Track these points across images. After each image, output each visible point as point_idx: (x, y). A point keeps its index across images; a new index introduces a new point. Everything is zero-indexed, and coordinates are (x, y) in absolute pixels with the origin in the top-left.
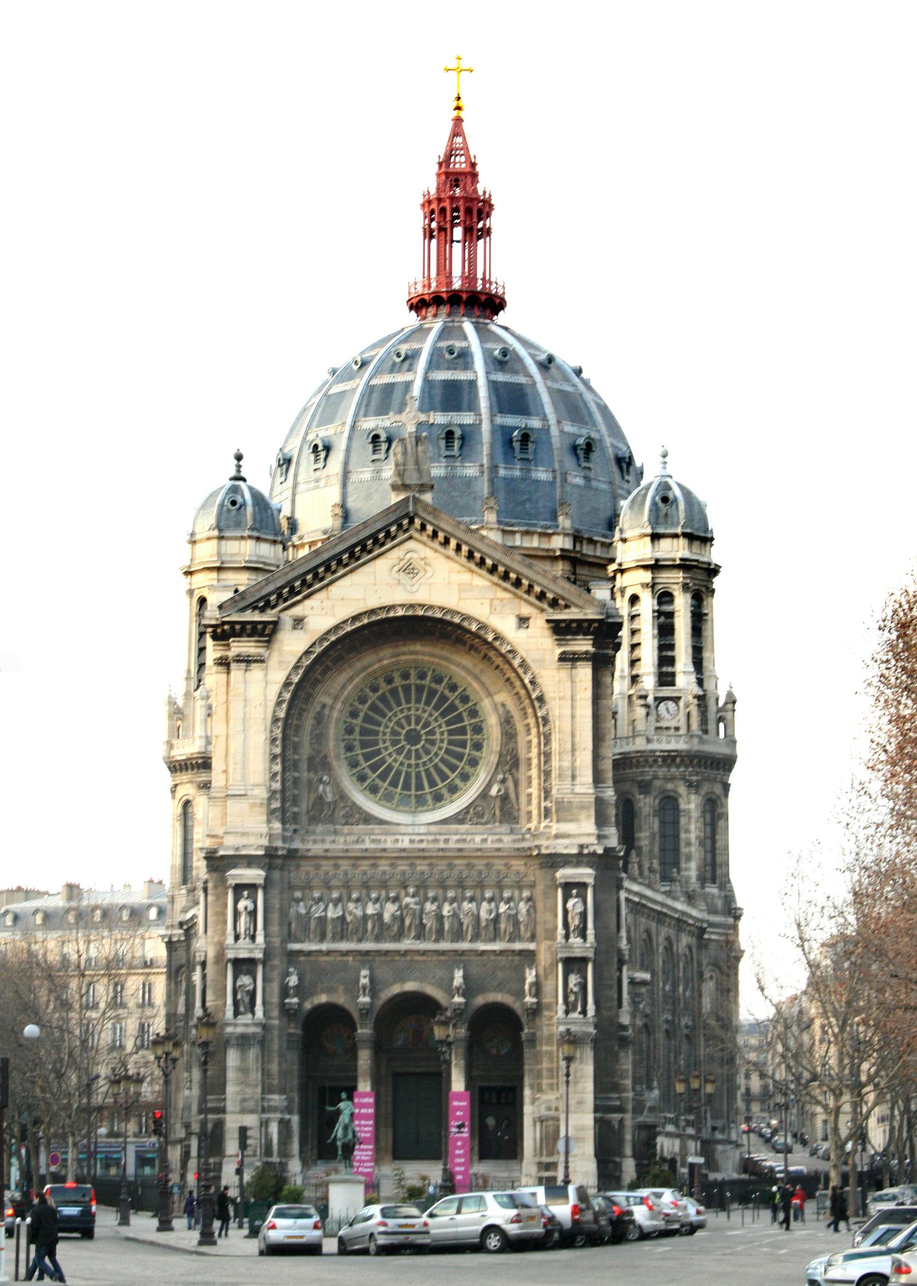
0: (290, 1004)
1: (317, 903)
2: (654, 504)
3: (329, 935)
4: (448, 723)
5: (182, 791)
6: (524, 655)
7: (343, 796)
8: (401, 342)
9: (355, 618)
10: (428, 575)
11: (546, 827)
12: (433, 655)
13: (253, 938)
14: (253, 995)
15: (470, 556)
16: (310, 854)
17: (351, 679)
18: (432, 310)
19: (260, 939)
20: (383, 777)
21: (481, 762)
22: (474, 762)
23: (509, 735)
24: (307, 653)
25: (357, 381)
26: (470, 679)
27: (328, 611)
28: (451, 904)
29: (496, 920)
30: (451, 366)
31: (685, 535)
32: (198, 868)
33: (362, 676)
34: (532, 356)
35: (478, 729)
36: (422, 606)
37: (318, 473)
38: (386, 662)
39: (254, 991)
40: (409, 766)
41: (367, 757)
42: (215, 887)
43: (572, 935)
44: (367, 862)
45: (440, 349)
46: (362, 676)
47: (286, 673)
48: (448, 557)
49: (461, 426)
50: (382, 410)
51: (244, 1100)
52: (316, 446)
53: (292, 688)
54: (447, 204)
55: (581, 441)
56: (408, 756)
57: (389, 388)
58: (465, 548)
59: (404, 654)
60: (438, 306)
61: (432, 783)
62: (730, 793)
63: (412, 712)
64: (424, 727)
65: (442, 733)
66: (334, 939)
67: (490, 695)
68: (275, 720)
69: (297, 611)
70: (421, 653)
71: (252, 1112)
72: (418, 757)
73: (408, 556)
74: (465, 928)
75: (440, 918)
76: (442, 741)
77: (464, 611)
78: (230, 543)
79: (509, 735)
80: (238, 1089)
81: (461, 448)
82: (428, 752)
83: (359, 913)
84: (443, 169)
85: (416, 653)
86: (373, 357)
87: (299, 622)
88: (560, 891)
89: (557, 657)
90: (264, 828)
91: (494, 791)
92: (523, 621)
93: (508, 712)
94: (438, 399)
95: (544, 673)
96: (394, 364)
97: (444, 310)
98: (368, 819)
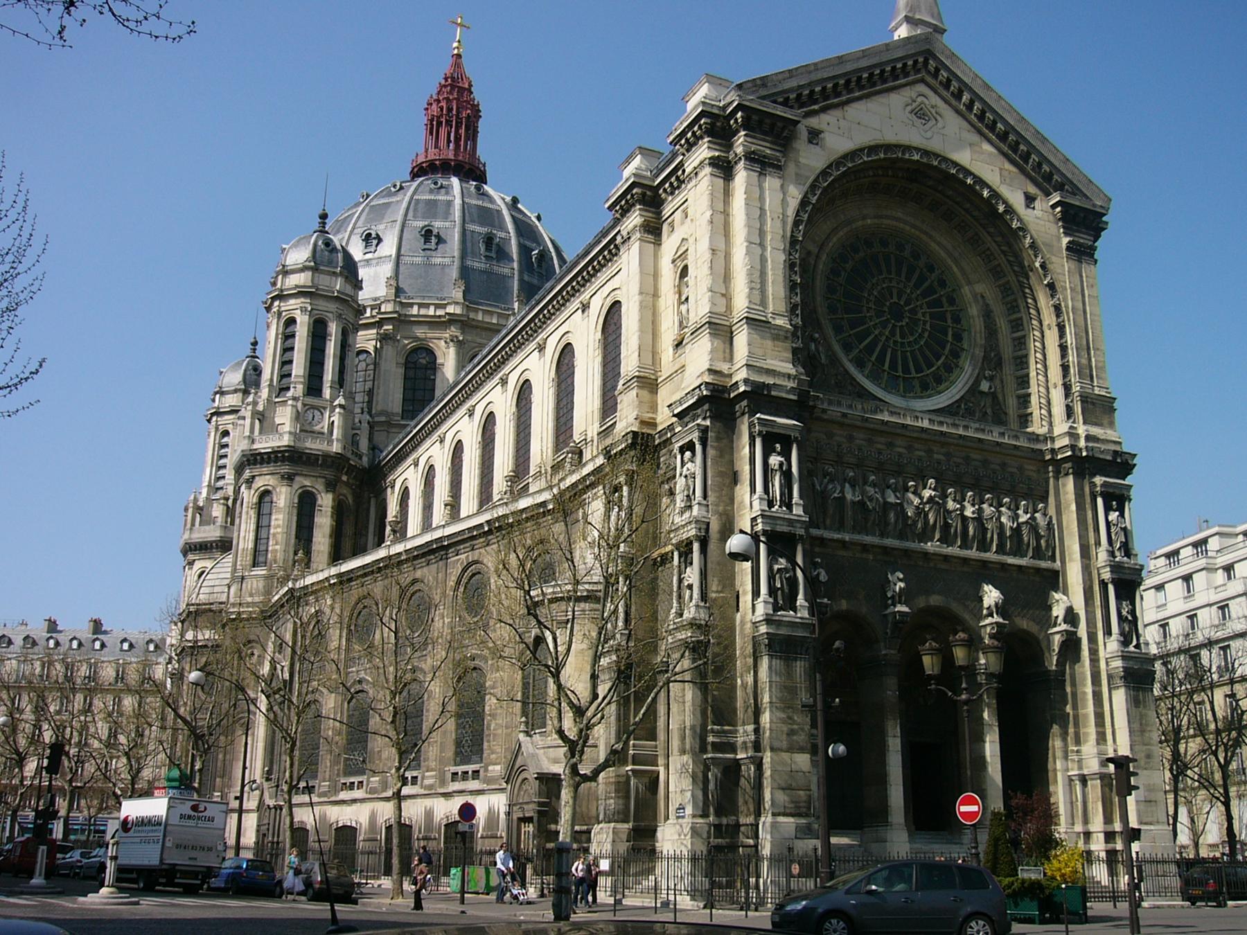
1: (831, 481)
3: (849, 522)
5: (260, 483)
6: (1035, 236)
7: (834, 360)
9: (873, 149)
10: (940, 125)
11: (1071, 427)
12: (913, 226)
13: (790, 507)
14: (793, 582)
15: (981, 117)
16: (826, 417)
17: (834, 230)
19: (798, 511)
20: (870, 349)
21: (963, 355)
22: (956, 354)
23: (991, 331)
24: (824, 173)
26: (949, 262)
28: (973, 505)
29: (1017, 531)
33: (845, 230)
35: (957, 320)
36: (937, 155)
37: (369, 256)
38: (869, 221)
40: (895, 342)
42: (718, 439)
43: (1117, 553)
44: (882, 440)
46: (845, 230)
47: (805, 188)
48: (958, 112)
51: (791, 733)
52: (370, 235)
53: (809, 208)
58: (977, 106)
59: (887, 217)
63: (894, 284)
64: (908, 303)
66: (854, 530)
67: (969, 283)
68: (793, 242)
69: (814, 122)
70: (900, 219)
71: (801, 750)
72: (902, 337)
73: (920, 99)
75: (964, 519)
76: (925, 323)
77: (977, 173)
78: (322, 276)
79: (991, 331)
80: (783, 716)
82: (912, 334)
85: (898, 219)
87: (814, 136)
88: (1100, 501)
89: (1064, 246)
90: (788, 368)
91: (985, 386)
92: (1030, 200)
93: (987, 305)
95: (1054, 259)
98: (863, 394)
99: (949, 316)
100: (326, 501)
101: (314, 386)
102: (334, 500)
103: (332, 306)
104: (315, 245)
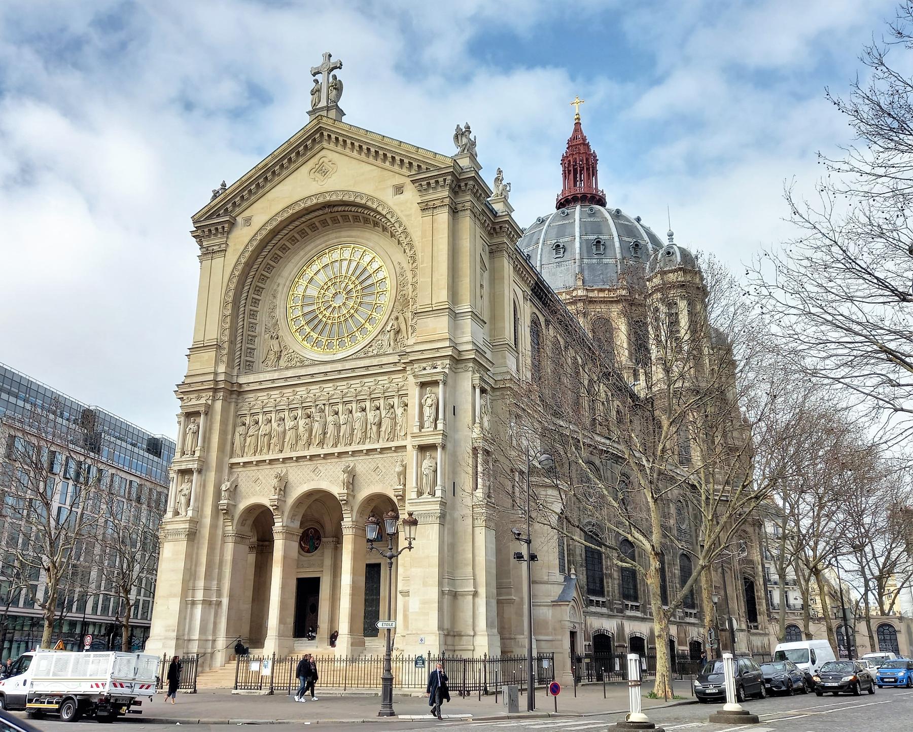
0: (223, 505)
27: (265, 212)
31: (680, 269)
47: (237, 257)
69: (247, 214)
83: (281, 429)
87: (248, 221)
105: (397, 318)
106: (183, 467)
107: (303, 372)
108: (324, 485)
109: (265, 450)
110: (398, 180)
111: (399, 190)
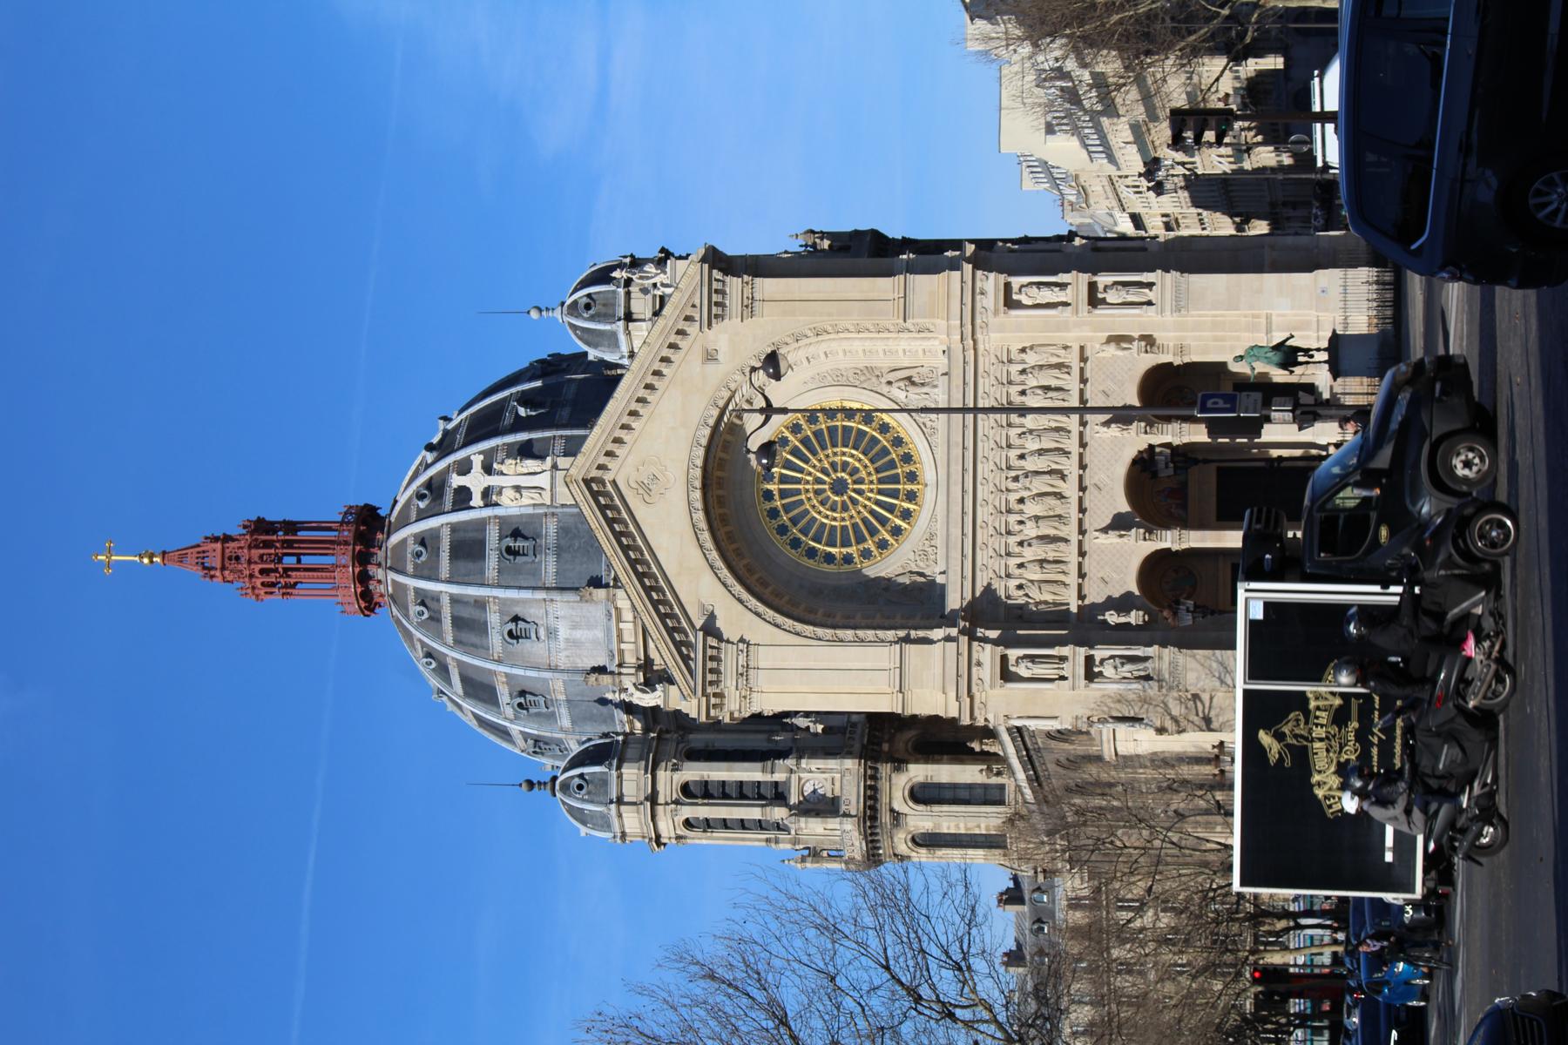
2: (592, 319)
3: (1061, 577)
4: (824, 448)
5: (902, 848)
8: (407, 616)
13: (1063, 659)
18: (372, 585)
25: (449, 660)
30: (436, 552)
32: (987, 828)
34: (428, 466)
39: (1121, 657)
41: (860, 539)
45: (416, 566)
49: (500, 539)
50: (481, 628)
52: (520, 705)
54: (257, 568)
55: (522, 412)
56: (860, 492)
57: (457, 622)
60: (371, 578)
61: (892, 465)
62: (912, 237)
65: (835, 454)
72: (861, 481)
74: (1054, 425)
81: (526, 538)
84: (218, 573)
86: (423, 644)
92: (710, 357)
94: (471, 566)
96: (430, 618)
97: (372, 569)
99: (830, 424)
100: (919, 772)
101: (778, 795)
102: (917, 762)
103: (663, 775)
104: (583, 800)
105: (889, 383)
106: (1081, 671)
107: (957, 509)
108: (1121, 470)
109: (1063, 567)
110: (696, 358)
111: (710, 357)
